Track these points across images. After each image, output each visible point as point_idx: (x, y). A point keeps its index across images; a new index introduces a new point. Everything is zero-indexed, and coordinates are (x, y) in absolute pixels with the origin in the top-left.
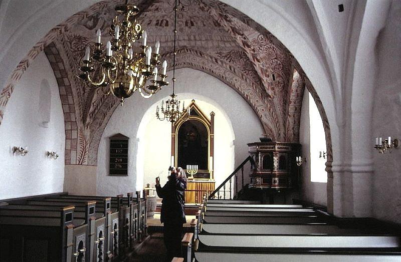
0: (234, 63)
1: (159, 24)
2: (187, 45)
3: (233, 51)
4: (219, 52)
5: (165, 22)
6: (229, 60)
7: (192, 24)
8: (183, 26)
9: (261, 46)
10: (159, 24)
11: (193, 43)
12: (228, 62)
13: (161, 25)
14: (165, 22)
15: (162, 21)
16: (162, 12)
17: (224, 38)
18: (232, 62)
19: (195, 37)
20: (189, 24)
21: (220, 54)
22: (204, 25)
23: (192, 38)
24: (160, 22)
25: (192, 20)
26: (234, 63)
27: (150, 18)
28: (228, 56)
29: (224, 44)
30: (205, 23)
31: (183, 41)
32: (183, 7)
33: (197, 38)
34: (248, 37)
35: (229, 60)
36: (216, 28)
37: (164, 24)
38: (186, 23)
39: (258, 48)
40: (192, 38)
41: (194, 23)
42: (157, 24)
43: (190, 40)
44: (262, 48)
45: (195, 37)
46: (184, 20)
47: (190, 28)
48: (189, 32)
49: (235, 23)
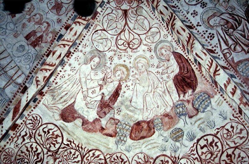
9: (30, 136)
17: (8, 60)
34: (39, 105)
36: (22, 38)
39: (23, 133)
44: (27, 141)
49: (61, 74)
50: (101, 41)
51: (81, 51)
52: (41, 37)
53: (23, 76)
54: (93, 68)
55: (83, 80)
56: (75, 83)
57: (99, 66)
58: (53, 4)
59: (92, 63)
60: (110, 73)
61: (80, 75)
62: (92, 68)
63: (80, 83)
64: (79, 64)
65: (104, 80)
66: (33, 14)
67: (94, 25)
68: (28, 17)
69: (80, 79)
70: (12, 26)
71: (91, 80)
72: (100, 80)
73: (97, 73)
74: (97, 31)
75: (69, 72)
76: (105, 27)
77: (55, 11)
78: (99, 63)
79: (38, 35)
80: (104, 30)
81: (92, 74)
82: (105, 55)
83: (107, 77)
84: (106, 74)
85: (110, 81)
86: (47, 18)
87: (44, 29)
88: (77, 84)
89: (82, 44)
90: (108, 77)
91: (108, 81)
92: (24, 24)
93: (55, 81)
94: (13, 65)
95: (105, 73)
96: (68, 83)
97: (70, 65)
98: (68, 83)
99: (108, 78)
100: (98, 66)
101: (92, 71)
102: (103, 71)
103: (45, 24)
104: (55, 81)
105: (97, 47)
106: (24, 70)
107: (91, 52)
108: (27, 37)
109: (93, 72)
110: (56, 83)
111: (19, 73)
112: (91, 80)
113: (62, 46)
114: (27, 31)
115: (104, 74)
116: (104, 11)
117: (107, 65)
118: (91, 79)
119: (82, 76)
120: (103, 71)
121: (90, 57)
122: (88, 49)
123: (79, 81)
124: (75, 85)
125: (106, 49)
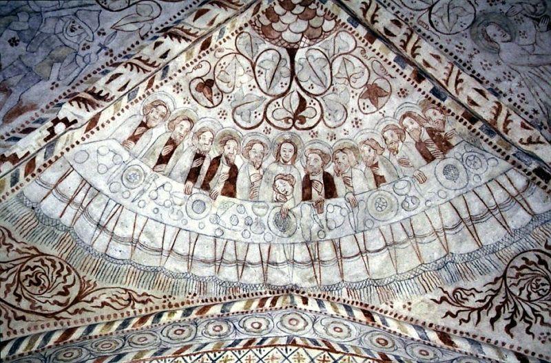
0: (537, 328)
1: (201, 178)
2: (306, 285)
3: (519, 263)
4: (450, 290)
5: (224, 169)
6: (502, 324)
7: (330, 191)
8: (289, 204)
10: (201, 178)
11: (329, 275)
12: (499, 334)
13: (205, 187)
14: (224, 169)
15: (216, 162)
16: (223, 114)
17: (471, 198)
18: (522, 325)
19: (337, 247)
20: (317, 192)
21: (458, 302)
22: (379, 180)
23: (327, 252)
24: (206, 166)
25: (330, 170)
26: (537, 328)
27: (172, 127)
28: (498, 301)
29: (474, 234)
30: (382, 171)
31: (287, 269)
32: (302, 105)
33: (348, 247)
35: (502, 324)
36: (428, 170)
37: (218, 185)
38: (308, 184)
40: (327, 252)
41: (338, 181)
42: (193, 175)
43: (314, 261)
45: (337, 247)
46: (299, 173)
47: (319, 206)
48: (315, 227)
50: (452, 18)
51: (471, 56)
52: (431, 132)
53: (512, 174)
54: (508, 37)
55: (533, 59)
56: (539, 77)
57: (507, 26)
58: (368, 102)
59: (498, 39)
60: (524, 5)
61: (523, 65)
62: (508, 41)
63: (541, 68)
64: (498, 63)
65: (538, 20)
66: (382, 144)
67: (419, 27)
68: (386, 153)
69: (530, 65)
70: (401, 184)
71: (535, 45)
72: (537, 28)
73: (520, 32)
74: (431, 22)
75: (514, 84)
76: (425, 6)
77: (381, 101)
78: (500, 27)
79: (426, 136)
80: (430, 9)
81: (522, 41)
82: (484, 14)
83: (533, 14)
84: (525, 15)
85: (543, 7)
86: (394, 117)
87: (416, 125)
88: (543, 72)
89: (456, 54)
90: (532, 9)
91: (541, 11)
92: (400, 162)
93: (531, 113)
94: (484, 192)
95: (523, 16)
96: (538, 89)
97: (498, 80)
98: (538, 89)
99: (536, 10)
100: (506, 28)
101: (516, 41)
102: (519, 20)
103: (406, 121)
104: (531, 113)
105: (465, 27)
106: (498, 170)
107: (475, 40)
108: (429, 158)
109: (519, 40)
110: (536, 112)
111: (503, 180)
112: (535, 45)
113: (459, 86)
114: (415, 157)
115: (525, 18)
116: (393, 4)
117: (505, 11)
118: (533, 44)
119: (525, 61)
120: (520, 21)
121: (485, 42)
122: (468, 43)
123: (536, 68)
124: (543, 76)
125: (470, 9)
